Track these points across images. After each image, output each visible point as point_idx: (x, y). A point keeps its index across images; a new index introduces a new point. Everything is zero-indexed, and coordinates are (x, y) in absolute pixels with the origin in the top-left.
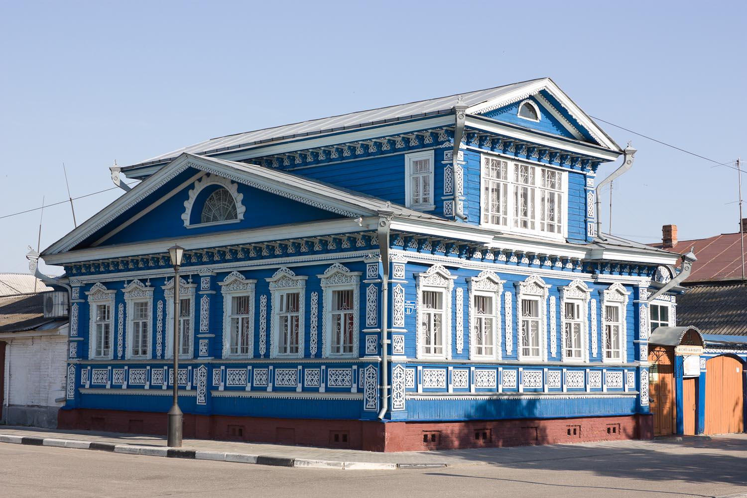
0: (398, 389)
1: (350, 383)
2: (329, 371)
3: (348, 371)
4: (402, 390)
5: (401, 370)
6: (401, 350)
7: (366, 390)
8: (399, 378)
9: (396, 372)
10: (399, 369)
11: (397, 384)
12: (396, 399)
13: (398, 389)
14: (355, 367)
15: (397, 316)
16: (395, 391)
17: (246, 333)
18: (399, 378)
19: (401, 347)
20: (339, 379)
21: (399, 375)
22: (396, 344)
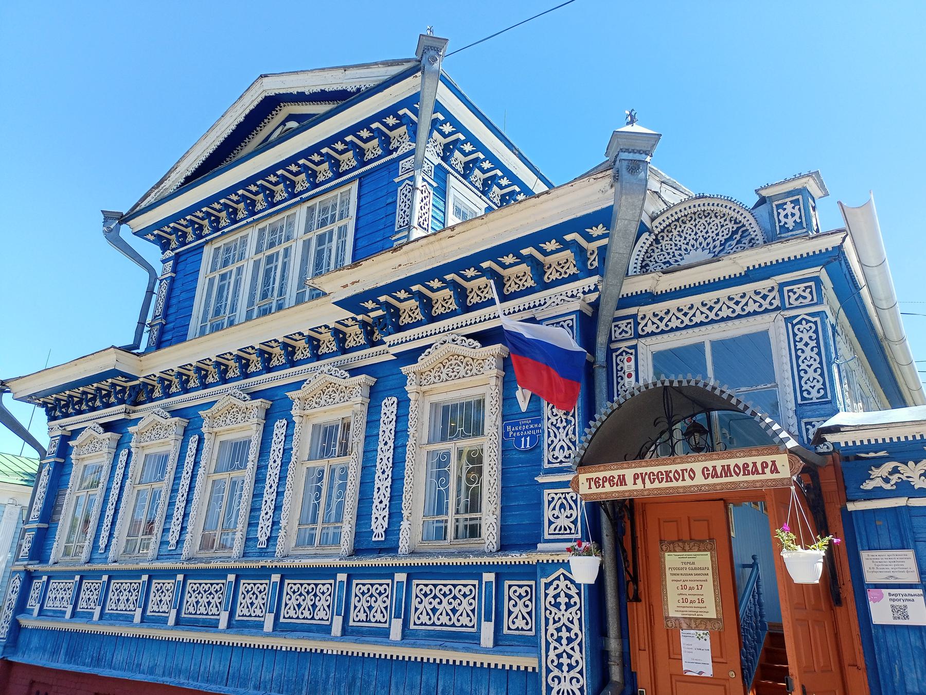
0: (564, 641)
1: (475, 620)
2: (354, 585)
3: (324, 585)
4: (575, 644)
5: (570, 585)
6: (572, 526)
7: (548, 644)
8: (563, 607)
9: (551, 592)
10: (562, 583)
11: (558, 625)
12: (556, 672)
13: (564, 641)
14: (489, 577)
15: (556, 441)
16: (552, 647)
17: (236, 508)
18: (563, 607)
19: (572, 519)
20: (440, 607)
21: (563, 600)
22: (556, 512)
